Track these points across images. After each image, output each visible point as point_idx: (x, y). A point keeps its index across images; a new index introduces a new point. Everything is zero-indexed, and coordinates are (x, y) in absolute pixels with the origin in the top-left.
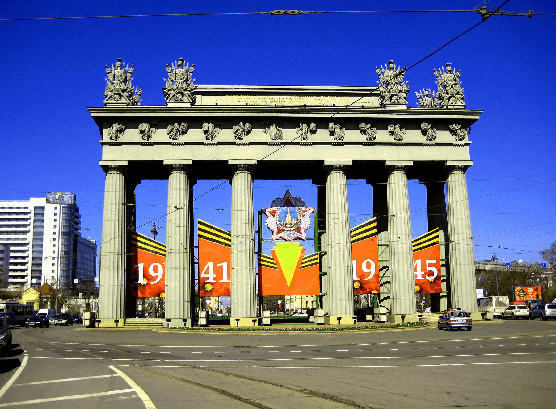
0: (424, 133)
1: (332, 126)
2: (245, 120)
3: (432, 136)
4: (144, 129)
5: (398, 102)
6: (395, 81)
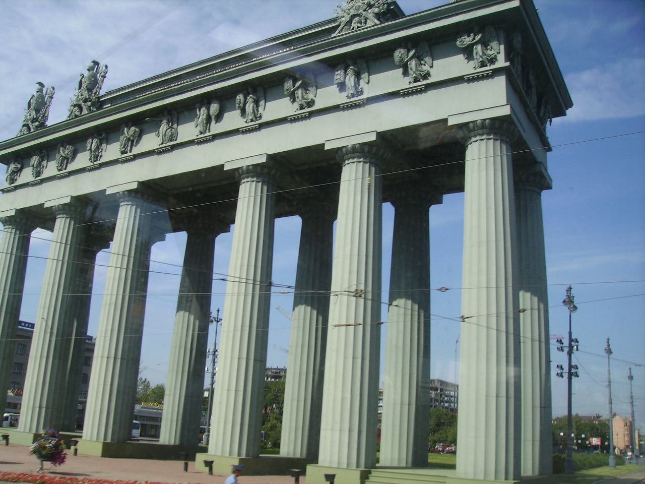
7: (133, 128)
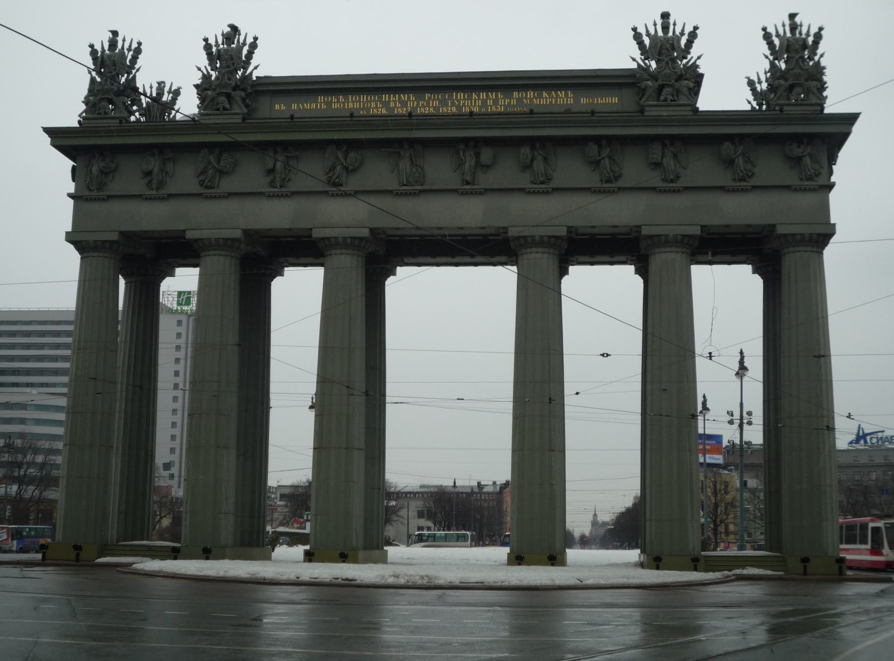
1: (525, 155)
3: (745, 172)
5: (674, 101)
6: (668, 56)
7: (352, 155)
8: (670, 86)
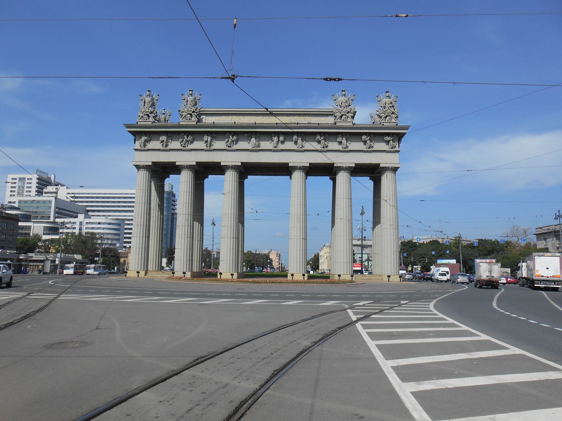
0: (365, 142)
2: (234, 133)
4: (163, 139)
8: (345, 115)
